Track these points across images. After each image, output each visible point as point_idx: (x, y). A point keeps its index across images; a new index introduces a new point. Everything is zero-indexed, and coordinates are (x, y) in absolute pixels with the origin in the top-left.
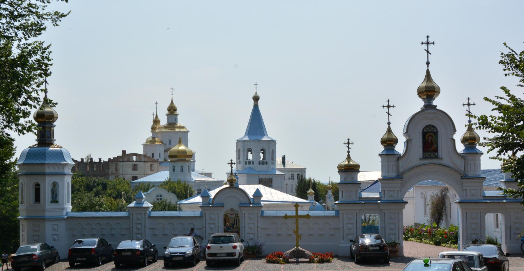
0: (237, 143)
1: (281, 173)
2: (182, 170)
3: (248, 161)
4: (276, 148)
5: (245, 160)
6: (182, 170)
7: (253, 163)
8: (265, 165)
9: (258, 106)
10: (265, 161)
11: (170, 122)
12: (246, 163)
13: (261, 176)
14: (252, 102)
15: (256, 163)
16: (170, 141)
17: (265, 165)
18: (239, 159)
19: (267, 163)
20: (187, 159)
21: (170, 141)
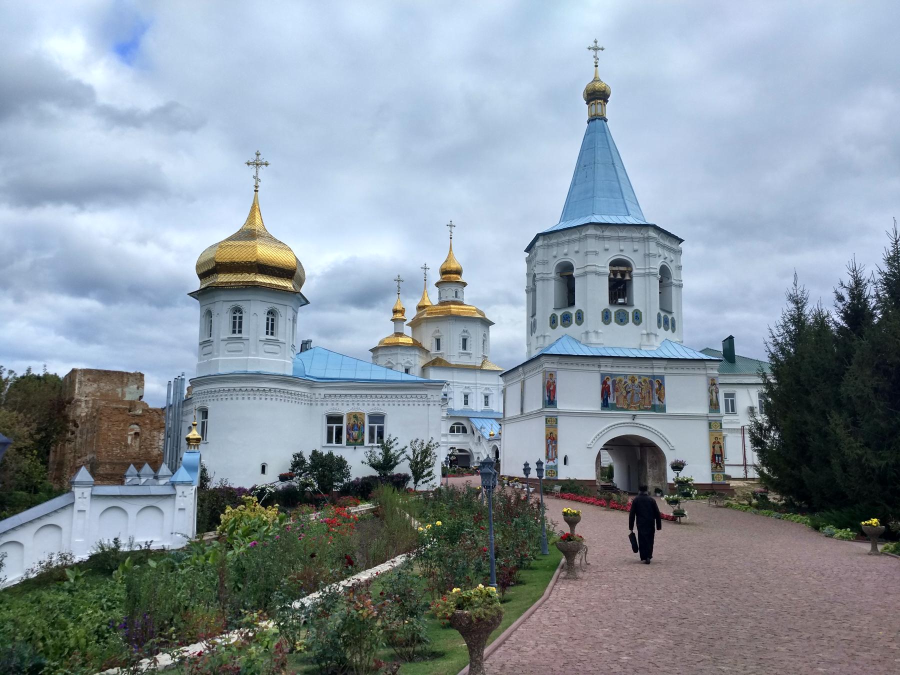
0: (529, 261)
1: (704, 357)
2: (237, 325)
3: (559, 314)
4: (680, 268)
5: (551, 311)
6: (237, 325)
7: (580, 317)
8: (631, 324)
9: (606, 121)
10: (630, 311)
11: (443, 299)
12: (553, 322)
13: (608, 368)
14: (583, 110)
15: (593, 317)
16: (438, 341)
17: (631, 324)
18: (534, 315)
19: (637, 318)
20: (262, 279)
21: (438, 341)
